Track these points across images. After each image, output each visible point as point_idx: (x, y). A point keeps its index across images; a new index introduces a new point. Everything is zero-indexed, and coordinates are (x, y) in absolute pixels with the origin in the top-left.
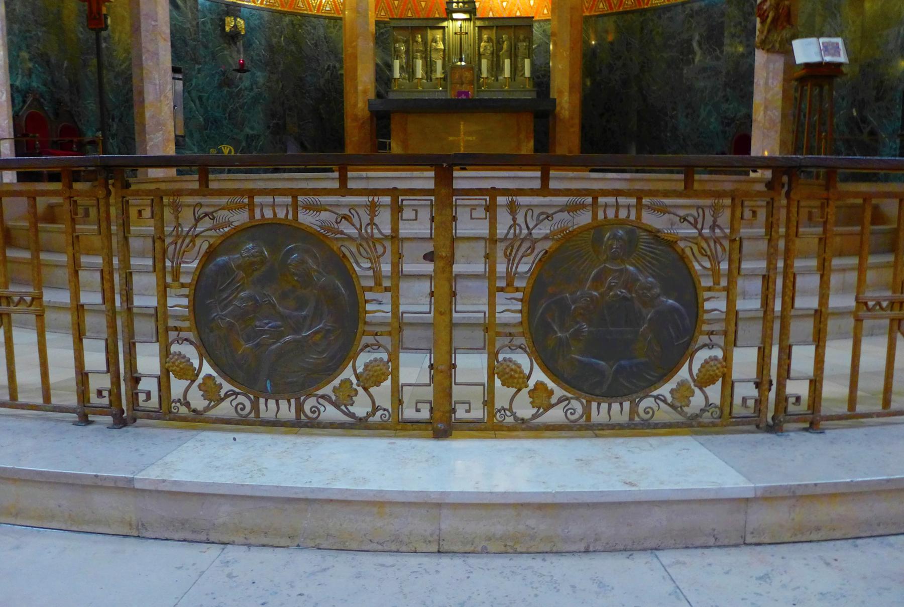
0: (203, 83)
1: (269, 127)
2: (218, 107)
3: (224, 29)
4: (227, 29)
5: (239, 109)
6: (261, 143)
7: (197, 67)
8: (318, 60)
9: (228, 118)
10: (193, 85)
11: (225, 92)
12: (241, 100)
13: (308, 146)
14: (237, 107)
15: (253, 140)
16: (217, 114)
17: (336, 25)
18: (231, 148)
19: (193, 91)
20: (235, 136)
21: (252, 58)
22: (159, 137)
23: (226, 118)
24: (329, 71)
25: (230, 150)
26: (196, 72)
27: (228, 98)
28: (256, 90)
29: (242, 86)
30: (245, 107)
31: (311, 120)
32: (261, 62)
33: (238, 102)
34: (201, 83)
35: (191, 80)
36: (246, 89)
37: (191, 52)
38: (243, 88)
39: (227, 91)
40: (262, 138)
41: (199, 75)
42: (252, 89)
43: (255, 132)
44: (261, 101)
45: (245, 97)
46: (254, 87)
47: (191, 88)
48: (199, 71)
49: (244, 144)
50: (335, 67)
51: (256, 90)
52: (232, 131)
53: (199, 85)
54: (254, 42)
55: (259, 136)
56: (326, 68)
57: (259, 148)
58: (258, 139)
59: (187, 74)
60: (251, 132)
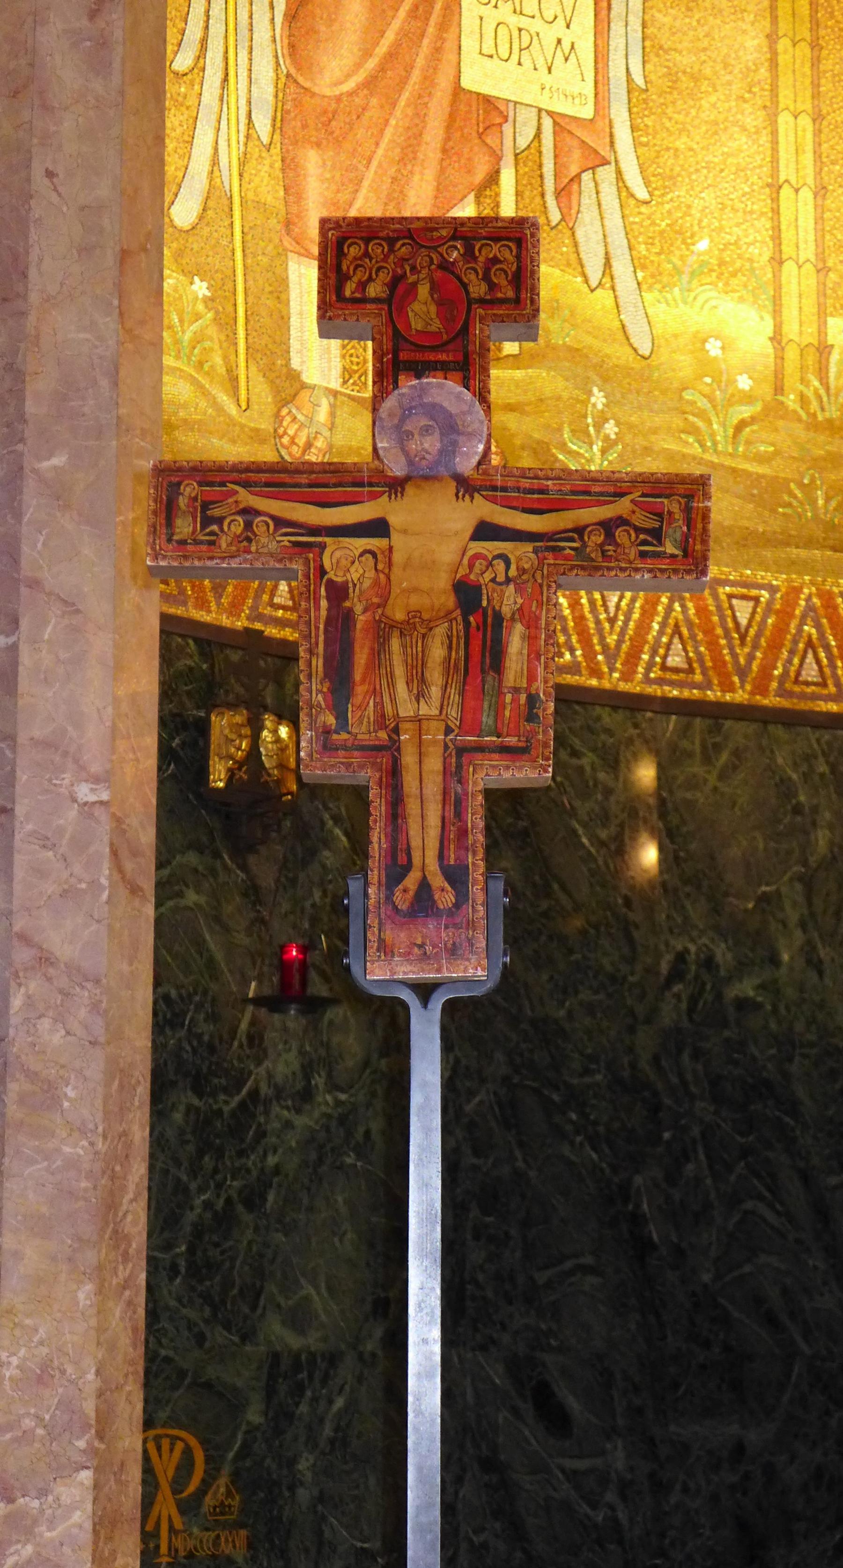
3: (203, 772)
4: (218, 779)
5: (240, 1208)
6: (339, 1403)
8: (627, 928)
9: (182, 1264)
12: (252, 1160)
13: (573, 1404)
14: (229, 1201)
15: (300, 1389)
17: (717, 748)
18: (193, 1442)
20: (211, 1372)
22: (72, 1508)
24: (677, 988)
25: (188, 1451)
27: (191, 1148)
28: (325, 1100)
30: (271, 1197)
31: (589, 1260)
33: (235, 1173)
36: (279, 1093)
38: (265, 1090)
39: (189, 1108)
40: (347, 1370)
42: (307, 1095)
43: (312, 1341)
46: (319, 1080)
49: (254, 1415)
50: (709, 963)
51: (325, 1100)
52: (200, 1339)
54: (327, 842)
55: (333, 1359)
56: (664, 968)
57: (328, 1431)
58: (325, 1380)
60: (294, 1342)
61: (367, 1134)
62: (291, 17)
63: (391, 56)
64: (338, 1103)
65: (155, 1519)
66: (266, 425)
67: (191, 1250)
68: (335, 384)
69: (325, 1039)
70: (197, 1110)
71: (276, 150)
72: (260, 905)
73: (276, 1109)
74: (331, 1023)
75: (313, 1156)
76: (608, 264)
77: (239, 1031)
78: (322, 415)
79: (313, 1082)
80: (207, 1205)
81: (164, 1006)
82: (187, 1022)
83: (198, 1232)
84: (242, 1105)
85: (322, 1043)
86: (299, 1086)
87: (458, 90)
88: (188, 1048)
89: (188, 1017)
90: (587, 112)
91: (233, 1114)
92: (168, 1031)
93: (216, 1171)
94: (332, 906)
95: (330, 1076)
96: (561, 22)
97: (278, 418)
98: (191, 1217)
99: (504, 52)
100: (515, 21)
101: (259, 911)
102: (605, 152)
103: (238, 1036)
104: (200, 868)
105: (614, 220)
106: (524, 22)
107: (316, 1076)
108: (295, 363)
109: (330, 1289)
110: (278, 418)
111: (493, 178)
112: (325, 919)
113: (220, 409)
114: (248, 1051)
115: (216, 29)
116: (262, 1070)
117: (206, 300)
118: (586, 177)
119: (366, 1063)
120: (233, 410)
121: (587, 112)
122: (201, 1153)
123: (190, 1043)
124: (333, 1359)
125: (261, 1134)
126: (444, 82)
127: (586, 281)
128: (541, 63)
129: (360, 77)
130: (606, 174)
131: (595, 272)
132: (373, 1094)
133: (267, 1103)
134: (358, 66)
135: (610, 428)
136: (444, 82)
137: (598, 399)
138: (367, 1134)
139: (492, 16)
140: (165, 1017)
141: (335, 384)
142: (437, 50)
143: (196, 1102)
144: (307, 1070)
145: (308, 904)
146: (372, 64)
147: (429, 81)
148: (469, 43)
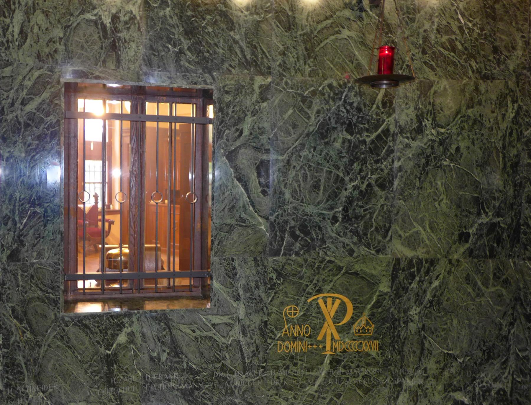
0: (274, 126)
1: (464, 237)
2: (316, 187)
5: (376, 189)
6: (436, 283)
7: (259, 80)
9: (340, 217)
10: (246, 132)
11: (338, 145)
14: (369, 185)
15: (413, 276)
16: (310, 209)
18: (346, 300)
19: (242, 150)
20: (357, 268)
21: (426, 39)
23: (335, 219)
26: (255, 97)
27: (346, 160)
28: (431, 133)
29: (389, 122)
30: (396, 182)
32: (454, 49)
34: (266, 125)
35: (240, 120)
36: (402, 131)
37: (243, 44)
38: (392, 129)
39: (344, 141)
40: (441, 268)
41: (265, 104)
42: (420, 130)
43: (421, 253)
44: (446, 162)
45: (397, 154)
46: (427, 123)
47: (238, 143)
48: (265, 90)
49: (384, 287)
51: (431, 133)
52: (351, 252)
53: (262, 131)
55: (432, 262)
57: (429, 296)
58: (427, 273)
59: (228, 105)
60: (409, 253)
61: (458, 149)
64: (439, 133)
65: (323, 334)
67: (346, 210)
69: (432, 101)
70: (350, 141)
72: (391, 33)
73: (400, 138)
74: (435, 92)
75: (423, 161)
77: (377, 100)
79: (423, 124)
80: (355, 188)
81: (328, 90)
82: (343, 97)
83: (350, 201)
84: (379, 137)
85: (430, 103)
86: (415, 126)
88: (344, 110)
89: (344, 95)
91: (373, 142)
92: (331, 102)
93: (361, 170)
94: (437, 30)
95: (434, 120)
98: (345, 194)
101: (390, 37)
103: (376, 102)
104: (352, 18)
107: (426, 120)
109: (431, 228)
112: (433, 37)
114: (382, 110)
116: (391, 119)
119: (458, 113)
122: (352, 162)
123: (345, 108)
124: (432, 262)
125: (391, 151)
132: (462, 128)
133: (394, 135)
138: (458, 149)
140: (329, 96)
143: (349, 137)
144: (420, 118)
145: (421, 31)
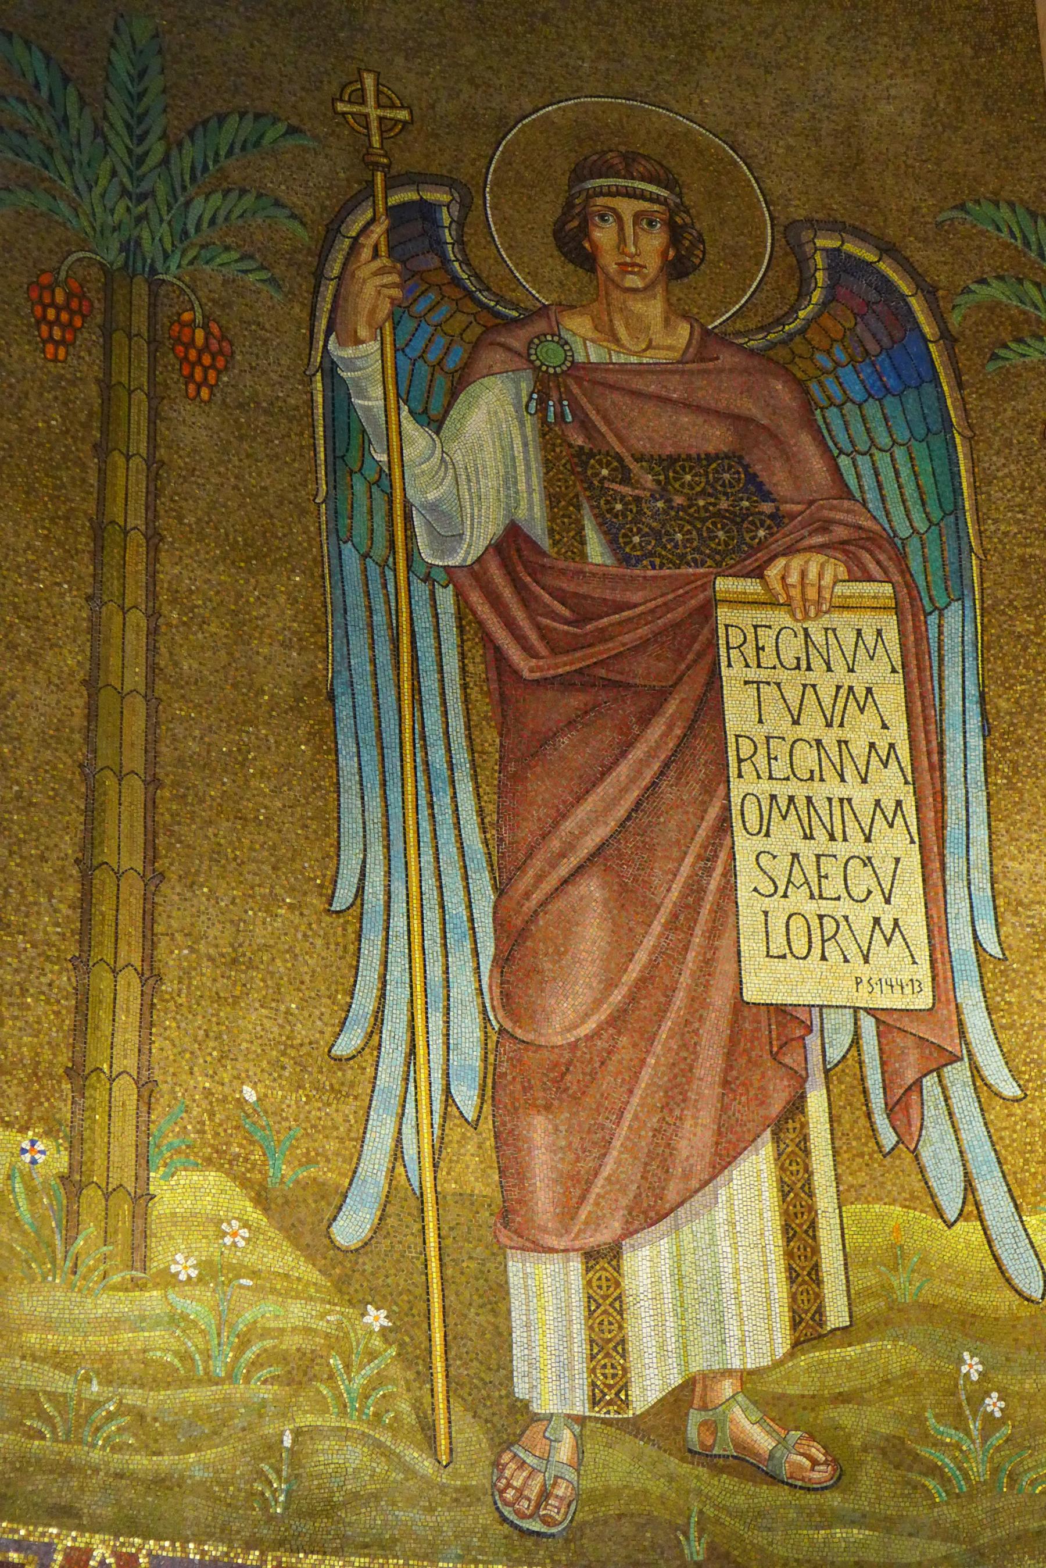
62: (503, 961)
63: (642, 982)
66: (479, 1478)
68: (580, 1407)
71: (487, 1126)
76: (969, 1186)
78: (565, 1451)
87: (740, 1004)
90: (924, 1000)
96: (877, 897)
97: (497, 1465)
99: (800, 946)
100: (811, 908)
102: (953, 1046)
105: (974, 1131)
106: (826, 907)
108: (521, 1390)
110: (497, 1465)
111: (797, 1105)
113: (409, 1470)
115: (397, 995)
117: (384, 1331)
118: (930, 1082)
120: (426, 1466)
121: (924, 1000)
126: (720, 999)
127: (939, 1212)
128: (853, 951)
129: (602, 1015)
130: (958, 1074)
131: (951, 1203)
134: (598, 1003)
135: (993, 1404)
136: (720, 999)
137: (972, 1367)
139: (779, 909)
141: (580, 1407)
142: (707, 963)
146: (617, 996)
147: (698, 1003)
148: (751, 946)
